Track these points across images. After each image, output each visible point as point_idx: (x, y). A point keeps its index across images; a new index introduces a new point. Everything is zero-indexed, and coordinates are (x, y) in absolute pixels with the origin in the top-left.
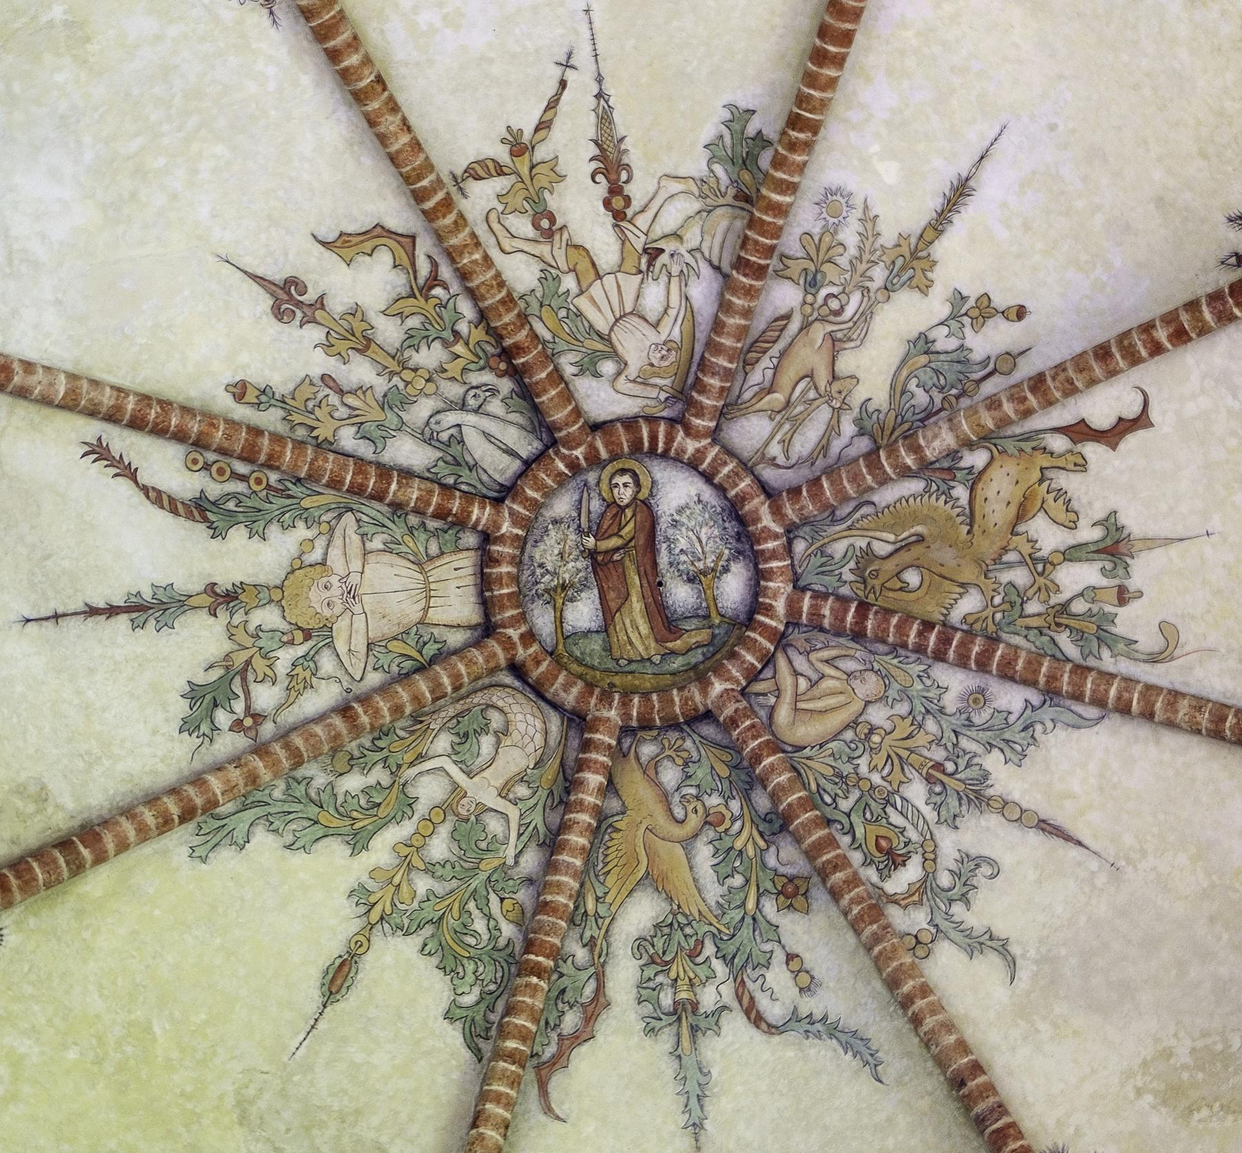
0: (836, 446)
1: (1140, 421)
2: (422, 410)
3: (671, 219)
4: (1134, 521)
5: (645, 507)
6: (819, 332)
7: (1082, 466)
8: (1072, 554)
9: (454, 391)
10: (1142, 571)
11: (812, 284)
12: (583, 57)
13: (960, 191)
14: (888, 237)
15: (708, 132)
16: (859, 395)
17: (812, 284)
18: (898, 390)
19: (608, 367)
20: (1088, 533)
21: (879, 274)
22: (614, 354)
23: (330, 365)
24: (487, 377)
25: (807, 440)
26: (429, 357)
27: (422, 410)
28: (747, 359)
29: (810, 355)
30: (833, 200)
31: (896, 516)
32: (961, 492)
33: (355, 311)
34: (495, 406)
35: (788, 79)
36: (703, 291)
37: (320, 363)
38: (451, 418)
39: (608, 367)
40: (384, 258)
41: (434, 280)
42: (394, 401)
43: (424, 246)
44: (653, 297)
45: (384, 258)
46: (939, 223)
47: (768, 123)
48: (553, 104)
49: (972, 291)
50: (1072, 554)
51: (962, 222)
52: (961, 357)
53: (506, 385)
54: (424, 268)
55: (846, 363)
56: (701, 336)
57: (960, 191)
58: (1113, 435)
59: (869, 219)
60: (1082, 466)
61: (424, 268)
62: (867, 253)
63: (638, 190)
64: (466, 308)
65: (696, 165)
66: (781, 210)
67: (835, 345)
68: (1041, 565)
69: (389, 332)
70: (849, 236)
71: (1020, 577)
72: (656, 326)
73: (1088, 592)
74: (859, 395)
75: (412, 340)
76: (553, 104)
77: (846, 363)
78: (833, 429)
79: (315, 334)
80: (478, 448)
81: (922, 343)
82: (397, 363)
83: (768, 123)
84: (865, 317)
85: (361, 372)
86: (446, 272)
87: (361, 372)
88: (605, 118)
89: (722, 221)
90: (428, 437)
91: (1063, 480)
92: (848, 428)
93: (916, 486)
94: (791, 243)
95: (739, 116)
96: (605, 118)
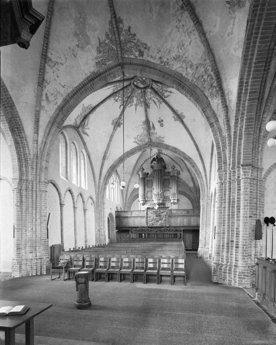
0: (134, 94)
1: (120, 108)
2: (160, 87)
3: (150, 101)
4: (116, 102)
5: (143, 85)
6: (139, 99)
7: (121, 103)
8: (118, 99)
9: (159, 89)
10: (114, 101)
11: (141, 101)
12: (159, 109)
13: (136, 110)
14: (138, 106)
15: (151, 107)
16: (135, 98)
17: (141, 101)
18: (133, 99)
19: (150, 92)
20: (118, 100)
21: (137, 104)
22: (150, 93)
23: (167, 89)
24: (157, 90)
25: (136, 93)
26: (161, 91)
27: (160, 87)
28: (142, 96)
29: (139, 98)
30: (142, 107)
31: (128, 93)
32: (126, 97)
33: (166, 92)
34: (156, 88)
35: (148, 112)
36: (147, 98)
37: (167, 89)
38: (158, 87)
39: (150, 92)
40: (166, 96)
41: (162, 95)
42: (162, 88)
43: (164, 97)
44: (149, 97)
45: (166, 96)
46: (136, 108)
47: (148, 109)
48: (160, 106)
49: (132, 106)
50: (118, 99)
51: (135, 109)
52: (130, 103)
53: (156, 90)
54: (163, 96)
55: (136, 98)
56: (146, 96)
57: (136, 110)
58: (121, 106)
59: (140, 106)
60: (121, 103)
61: (163, 96)
62: (139, 104)
63: (153, 102)
64: (160, 94)
65: (150, 105)
66: (144, 105)
67: (138, 99)
68: (119, 97)
69: (164, 92)
70: (140, 105)
71: (120, 95)
72: (148, 95)
73: (116, 98)
74: (135, 98)
75: (162, 92)
76: (160, 106)
77: (136, 98)
78: (135, 95)
79: (169, 90)
80: (155, 85)
81: (133, 102)
82: (163, 90)
83: (148, 109)
84: (137, 101)
85: (165, 89)
86: (162, 96)
87: (165, 89)
88: (156, 105)
89: (147, 102)
90: (159, 86)
91: (121, 102)
92: (134, 95)
93: (129, 95)
94: (143, 103)
95: (149, 108)
96: (156, 105)
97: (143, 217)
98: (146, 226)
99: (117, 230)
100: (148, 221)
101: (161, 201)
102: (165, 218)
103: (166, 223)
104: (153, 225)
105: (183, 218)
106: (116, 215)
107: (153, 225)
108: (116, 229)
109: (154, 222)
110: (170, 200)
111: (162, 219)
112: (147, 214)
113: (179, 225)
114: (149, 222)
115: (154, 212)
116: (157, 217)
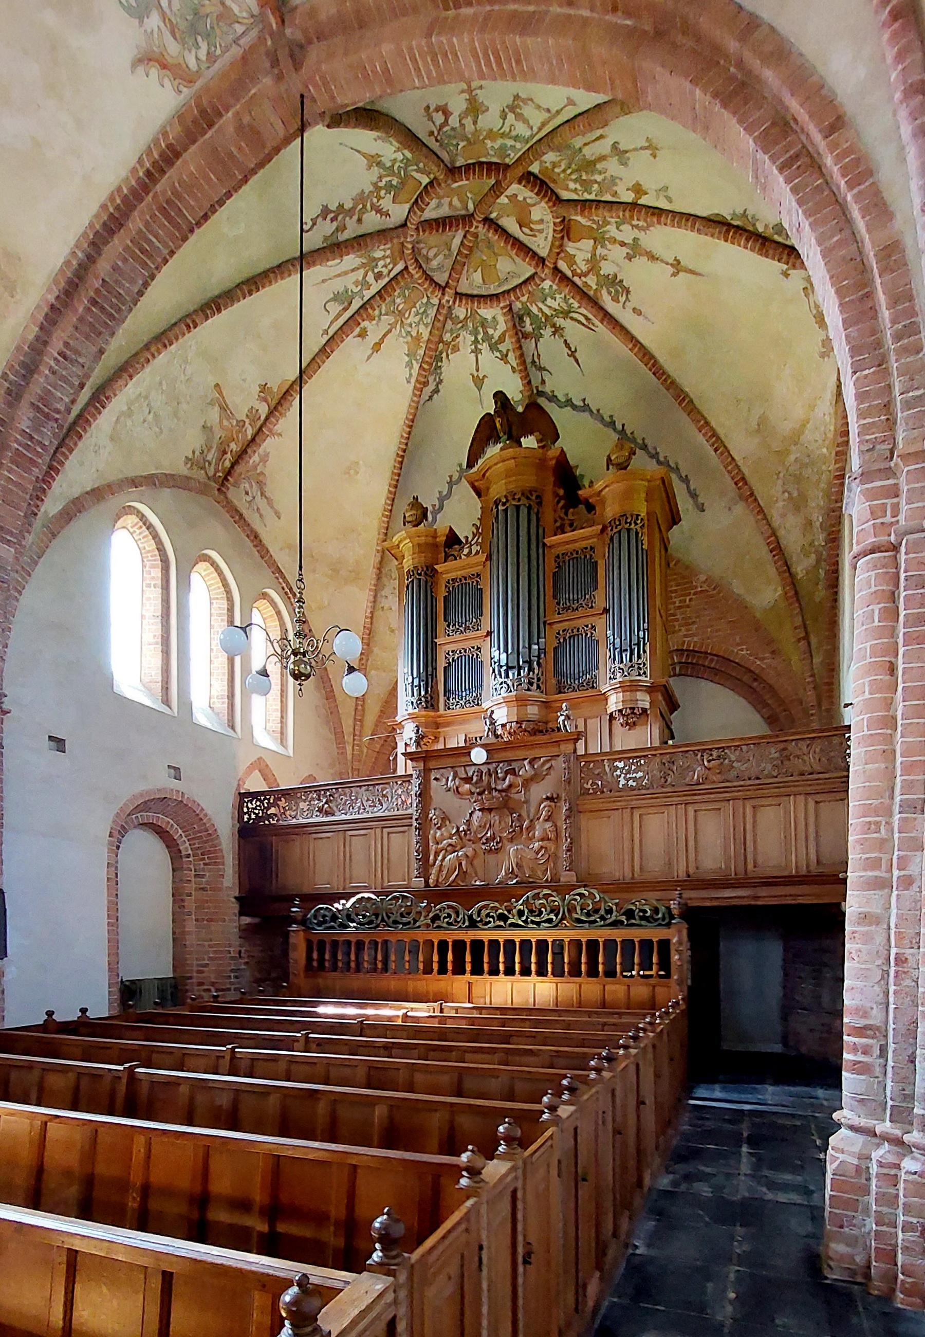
97: (400, 821)
98: (418, 883)
99: (247, 920)
100: (433, 847)
101: (533, 711)
102: (548, 825)
103: (556, 856)
104: (463, 874)
105: (691, 809)
106: (240, 818)
107: (463, 874)
108: (242, 913)
109: (470, 860)
110: (604, 697)
111: (531, 827)
112: (424, 795)
113: (655, 867)
114: (437, 854)
115: (468, 780)
116: (495, 818)
